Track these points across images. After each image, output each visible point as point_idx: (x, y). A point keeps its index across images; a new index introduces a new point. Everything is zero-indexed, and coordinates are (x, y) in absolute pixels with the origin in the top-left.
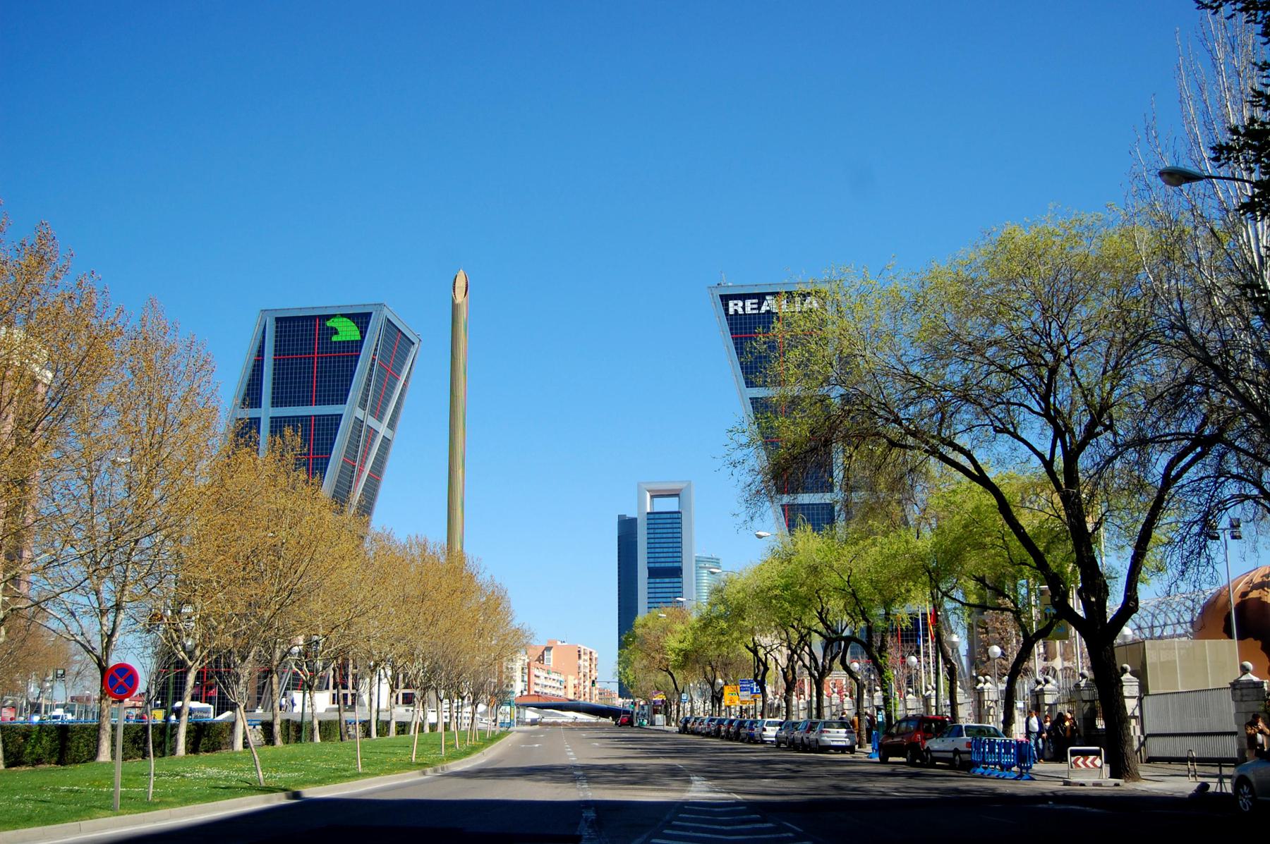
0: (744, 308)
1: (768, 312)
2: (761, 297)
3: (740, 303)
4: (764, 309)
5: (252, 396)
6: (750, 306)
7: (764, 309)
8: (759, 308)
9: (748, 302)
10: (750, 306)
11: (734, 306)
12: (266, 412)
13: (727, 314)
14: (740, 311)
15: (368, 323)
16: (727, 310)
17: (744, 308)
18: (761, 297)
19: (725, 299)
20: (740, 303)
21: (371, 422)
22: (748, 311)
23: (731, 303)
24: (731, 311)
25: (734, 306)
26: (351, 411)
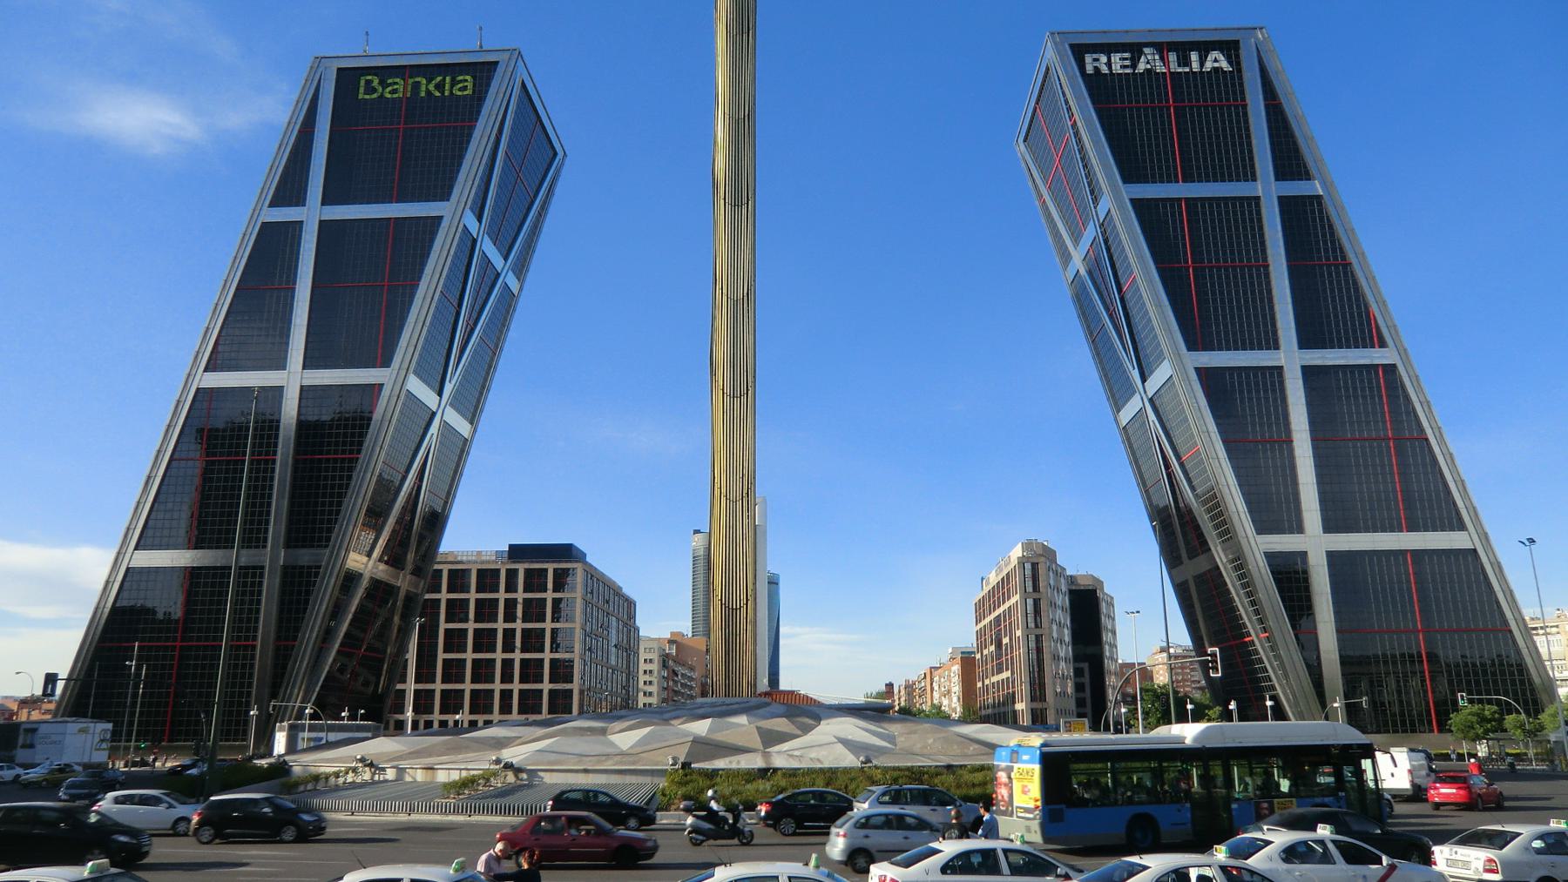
0: (1109, 64)
2: (1135, 50)
3: (1104, 59)
4: (1142, 67)
5: (289, 189)
6: (1118, 63)
7: (1142, 67)
8: (1134, 66)
9: (1116, 58)
10: (1118, 63)
11: (1096, 62)
12: (311, 214)
14: (1105, 70)
15: (490, 79)
17: (1109, 64)
18: (1135, 50)
20: (1104, 59)
21: (488, 247)
22: (1117, 69)
23: (1088, 58)
24: (1090, 69)
25: (1096, 62)
26: (455, 214)
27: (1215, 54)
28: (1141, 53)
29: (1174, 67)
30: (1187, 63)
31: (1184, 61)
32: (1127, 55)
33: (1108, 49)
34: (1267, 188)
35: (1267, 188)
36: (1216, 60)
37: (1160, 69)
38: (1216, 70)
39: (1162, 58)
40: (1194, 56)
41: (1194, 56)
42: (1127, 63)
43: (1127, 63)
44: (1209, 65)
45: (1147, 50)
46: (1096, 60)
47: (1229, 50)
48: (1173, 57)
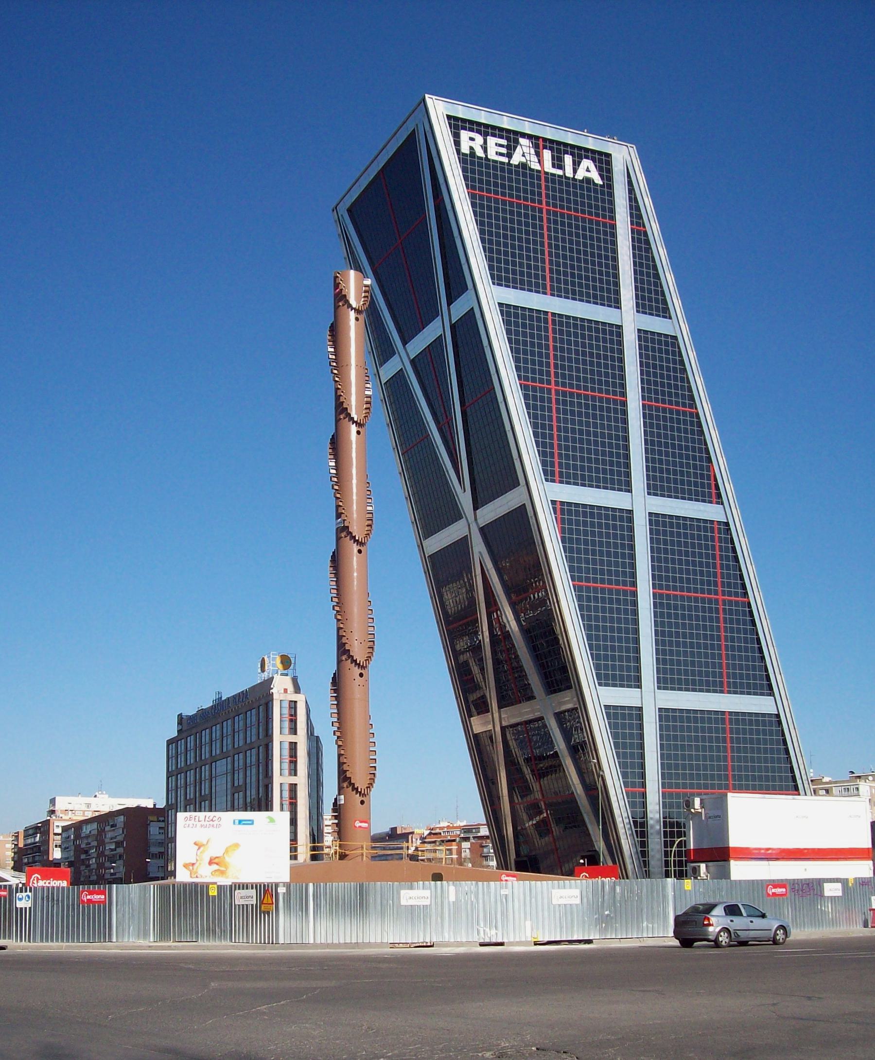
1: (524, 166)
3: (479, 139)
4: (517, 159)
6: (494, 148)
7: (517, 159)
8: (509, 156)
9: (492, 141)
10: (494, 148)
13: (458, 151)
14: (480, 153)
16: (457, 143)
18: (512, 138)
19: (457, 124)
22: (492, 155)
23: (465, 135)
24: (465, 149)
27: (586, 163)
28: (517, 142)
29: (548, 167)
30: (561, 167)
31: (558, 163)
32: (504, 142)
33: (486, 130)
34: (629, 319)
35: (629, 319)
36: (588, 170)
37: (536, 166)
38: (588, 180)
39: (538, 154)
40: (568, 160)
41: (568, 160)
42: (504, 151)
43: (504, 150)
44: (580, 175)
45: (523, 141)
46: (472, 139)
47: (601, 161)
48: (547, 155)
